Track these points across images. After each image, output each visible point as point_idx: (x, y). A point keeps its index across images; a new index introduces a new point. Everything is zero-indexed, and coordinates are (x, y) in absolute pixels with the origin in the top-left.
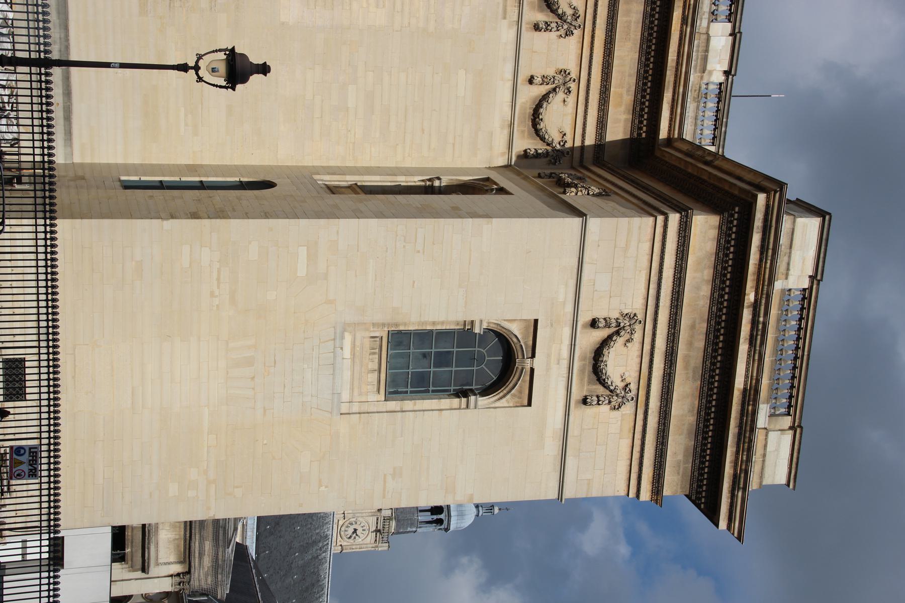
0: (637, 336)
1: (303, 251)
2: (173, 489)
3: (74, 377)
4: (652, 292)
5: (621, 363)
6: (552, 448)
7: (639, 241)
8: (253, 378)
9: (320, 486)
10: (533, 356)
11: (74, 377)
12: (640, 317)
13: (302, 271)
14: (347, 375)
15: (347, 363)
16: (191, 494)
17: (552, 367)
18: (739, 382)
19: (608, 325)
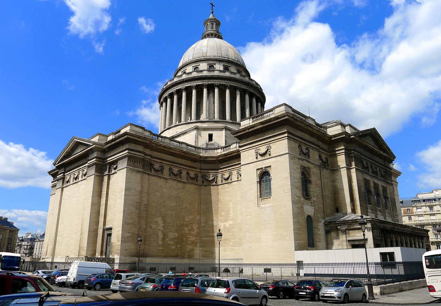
0: (258, 148)
1: (247, 217)
2: (288, 238)
3: (267, 259)
4: (251, 148)
5: (263, 150)
6: (279, 158)
7: (244, 154)
8: (267, 224)
9: (287, 207)
10: (262, 168)
11: (267, 259)
12: (255, 149)
13: (249, 217)
14: (267, 205)
15: (265, 205)
16: (288, 234)
17: (263, 164)
18: (261, 126)
19: (257, 155)
